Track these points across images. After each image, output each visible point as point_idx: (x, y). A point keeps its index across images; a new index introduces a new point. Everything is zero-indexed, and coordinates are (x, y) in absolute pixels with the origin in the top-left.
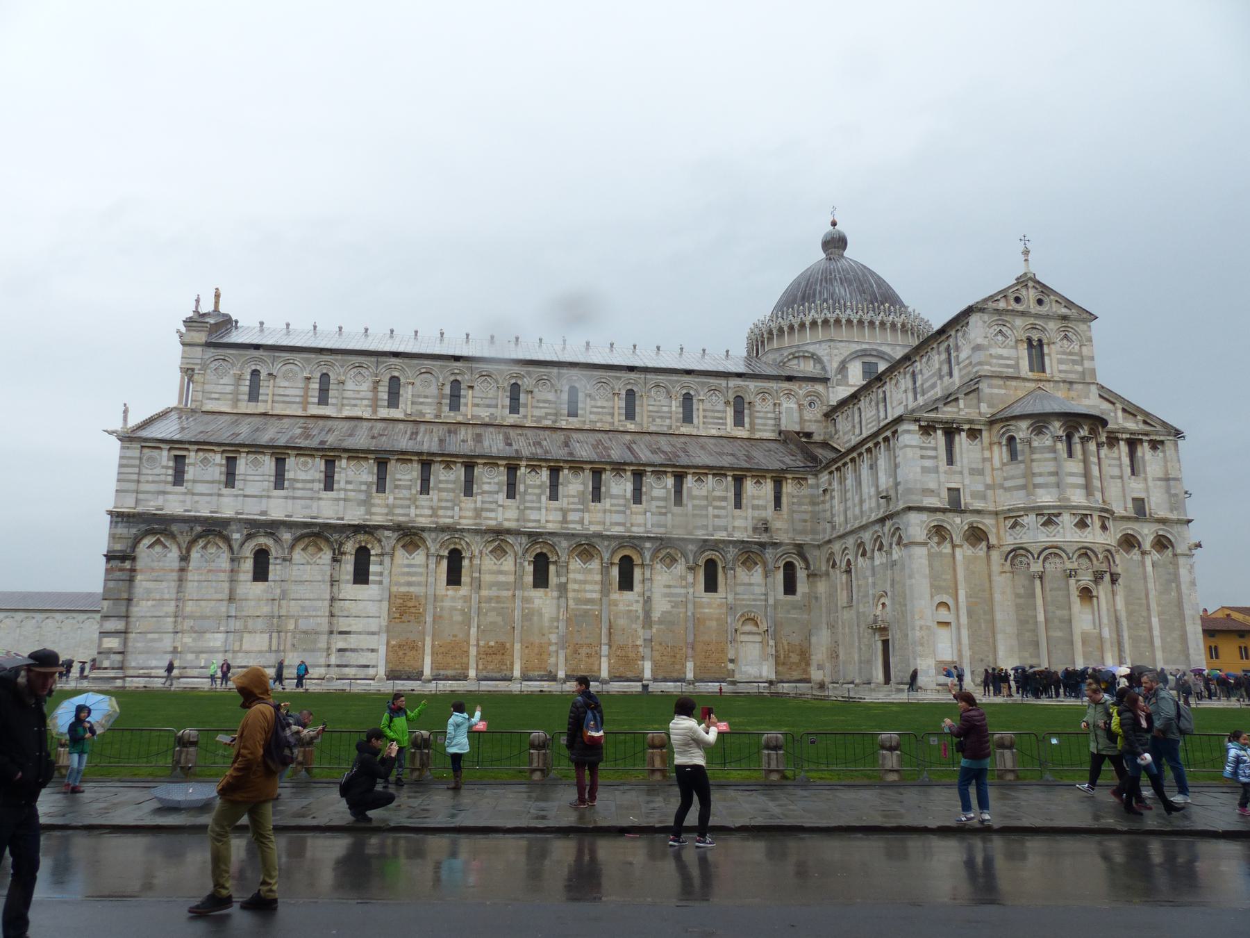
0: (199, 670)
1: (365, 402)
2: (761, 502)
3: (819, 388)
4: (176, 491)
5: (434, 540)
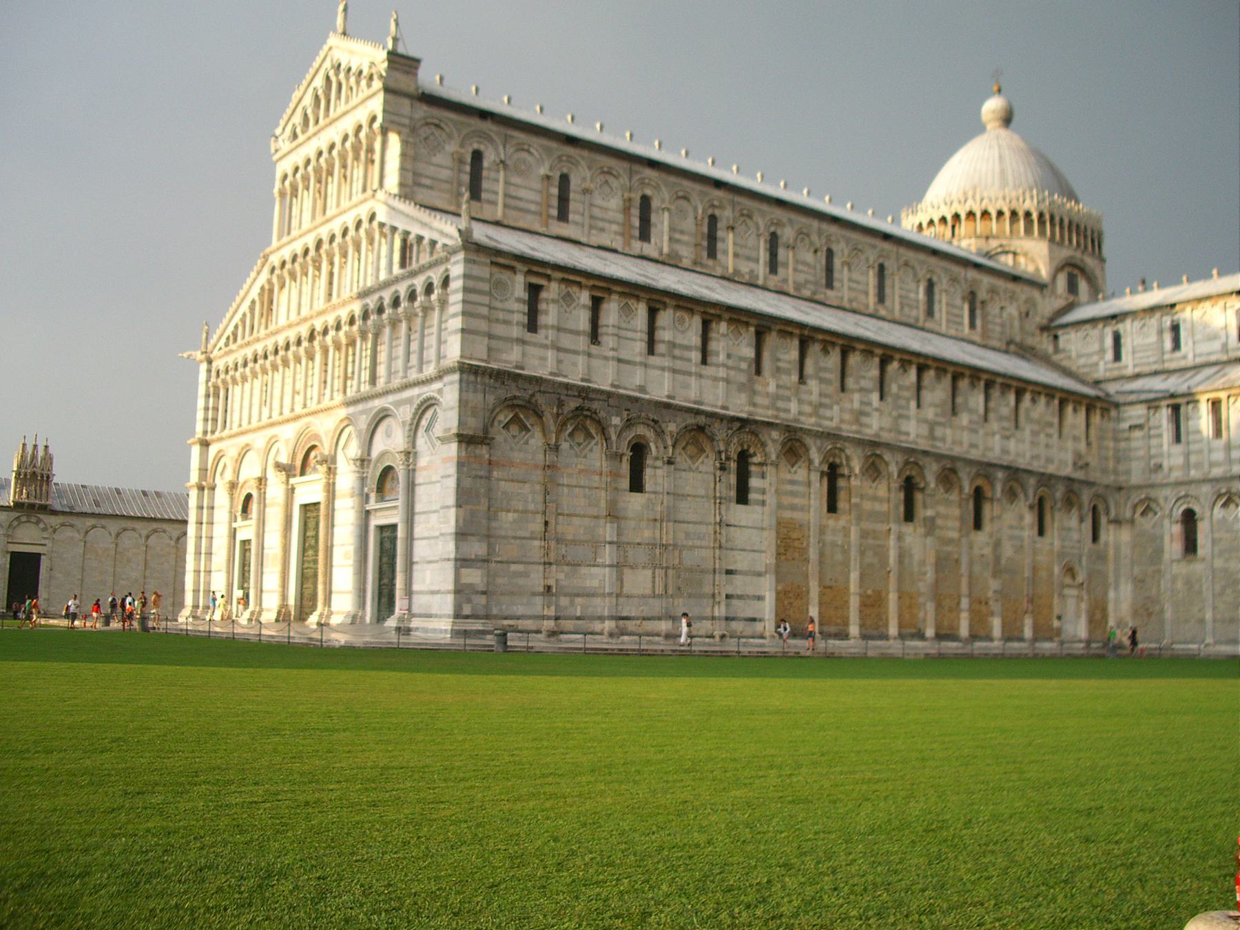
0: (573, 622)
1: (614, 227)
2: (1076, 432)
3: (1036, 294)
4: (533, 340)
5: (819, 450)
